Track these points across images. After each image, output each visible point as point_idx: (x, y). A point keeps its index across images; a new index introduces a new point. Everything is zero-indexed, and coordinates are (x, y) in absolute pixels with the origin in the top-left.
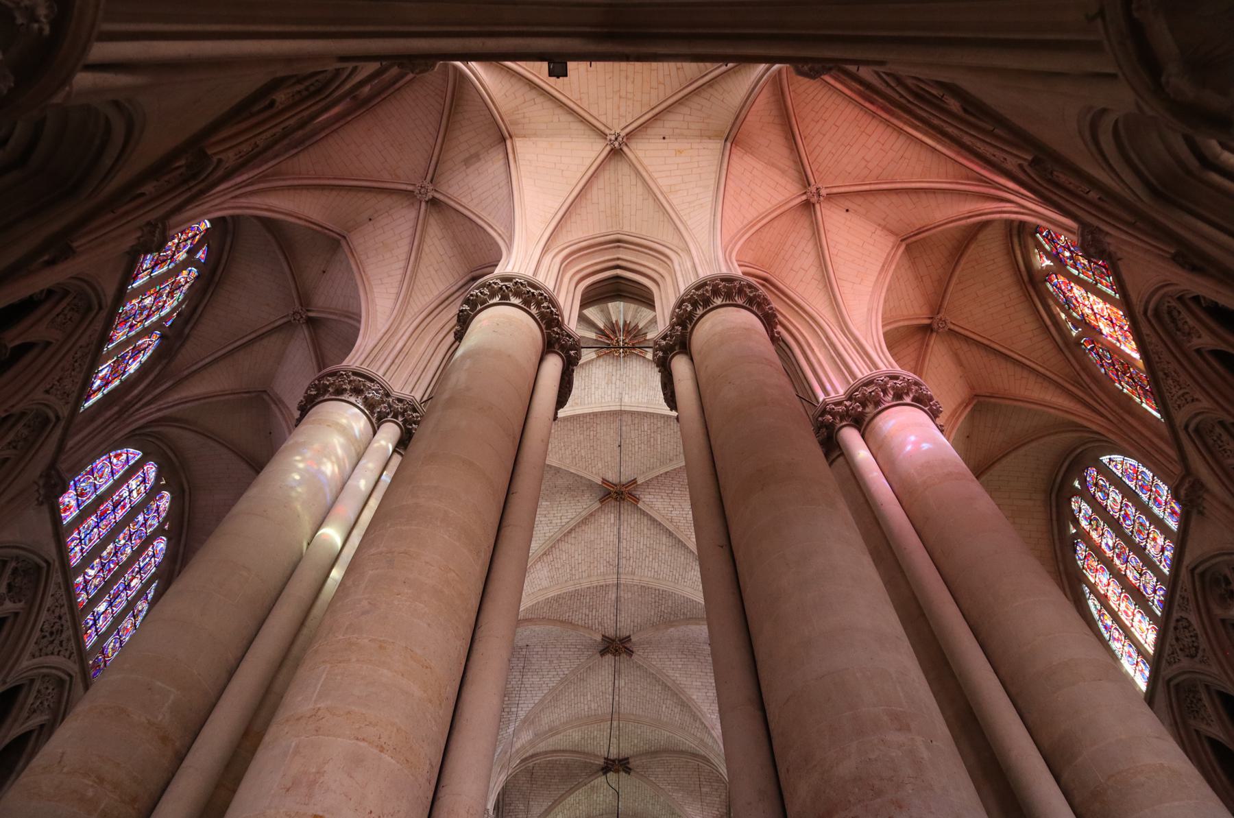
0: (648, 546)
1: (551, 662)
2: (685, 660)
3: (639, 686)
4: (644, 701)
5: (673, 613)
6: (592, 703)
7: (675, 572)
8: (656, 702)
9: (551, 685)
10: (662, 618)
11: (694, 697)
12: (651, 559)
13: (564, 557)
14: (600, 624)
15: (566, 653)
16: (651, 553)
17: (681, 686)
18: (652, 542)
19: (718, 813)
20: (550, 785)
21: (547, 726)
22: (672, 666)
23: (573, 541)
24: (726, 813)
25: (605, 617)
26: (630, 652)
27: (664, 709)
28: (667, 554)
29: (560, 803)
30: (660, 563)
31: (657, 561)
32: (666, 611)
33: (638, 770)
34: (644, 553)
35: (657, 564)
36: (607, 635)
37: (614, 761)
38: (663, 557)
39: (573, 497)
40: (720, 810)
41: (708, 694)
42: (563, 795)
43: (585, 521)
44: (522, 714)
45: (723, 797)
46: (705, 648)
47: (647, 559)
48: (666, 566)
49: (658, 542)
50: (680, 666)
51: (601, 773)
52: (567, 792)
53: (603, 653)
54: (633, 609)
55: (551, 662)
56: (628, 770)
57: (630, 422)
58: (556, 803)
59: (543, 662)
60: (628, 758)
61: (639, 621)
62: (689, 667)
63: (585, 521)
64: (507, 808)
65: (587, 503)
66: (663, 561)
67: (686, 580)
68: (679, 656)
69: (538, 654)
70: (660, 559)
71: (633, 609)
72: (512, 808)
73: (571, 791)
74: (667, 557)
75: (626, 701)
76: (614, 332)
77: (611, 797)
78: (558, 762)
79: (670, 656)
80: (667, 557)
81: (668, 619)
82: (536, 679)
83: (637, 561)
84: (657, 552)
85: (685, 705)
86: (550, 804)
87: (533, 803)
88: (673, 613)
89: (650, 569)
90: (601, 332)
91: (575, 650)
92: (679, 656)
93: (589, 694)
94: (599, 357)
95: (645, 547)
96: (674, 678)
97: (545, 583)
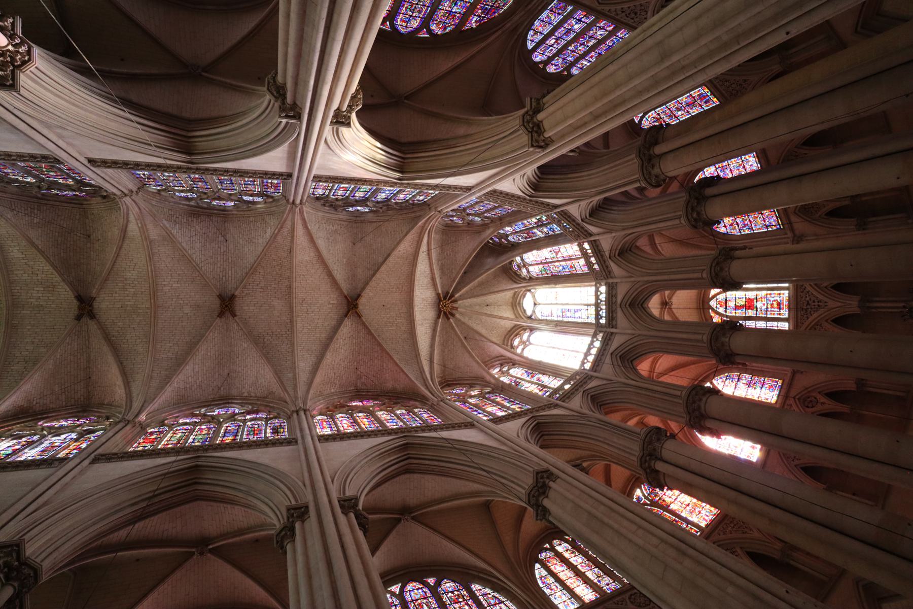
1: (211, 257)
6: (169, 288)
9: (194, 257)
11: (187, 367)
13: (313, 271)
14: (248, 294)
15: (218, 269)
17: (195, 356)
19: (34, 404)
20: (57, 248)
21: (157, 251)
22: (209, 348)
23: (322, 277)
24: (35, 412)
26: (221, 315)
29: (43, 256)
32: (265, 340)
33: (77, 327)
36: (237, 299)
37: (91, 306)
39: (349, 278)
40: (38, 405)
42: (50, 259)
43: (334, 282)
44: (174, 232)
45: (51, 406)
46: (226, 371)
50: (209, 354)
51: (77, 295)
52: (53, 263)
53: (220, 297)
54: (263, 317)
55: (211, 257)
56: (79, 318)
57: (401, 311)
58: (41, 252)
59: (211, 251)
60: (95, 318)
62: (209, 361)
63: (334, 282)
64: (36, 207)
65: (345, 286)
69: (218, 247)
71: (263, 317)
72: (36, 211)
73: (53, 265)
76: (451, 302)
77: (36, 303)
78: (82, 257)
79: (216, 346)
82: (198, 245)
85: (180, 362)
86: (40, 247)
87: (40, 231)
90: (452, 296)
91: (221, 276)
92: (217, 353)
93: (179, 285)
94: (438, 295)
96: (200, 350)
97: (299, 258)
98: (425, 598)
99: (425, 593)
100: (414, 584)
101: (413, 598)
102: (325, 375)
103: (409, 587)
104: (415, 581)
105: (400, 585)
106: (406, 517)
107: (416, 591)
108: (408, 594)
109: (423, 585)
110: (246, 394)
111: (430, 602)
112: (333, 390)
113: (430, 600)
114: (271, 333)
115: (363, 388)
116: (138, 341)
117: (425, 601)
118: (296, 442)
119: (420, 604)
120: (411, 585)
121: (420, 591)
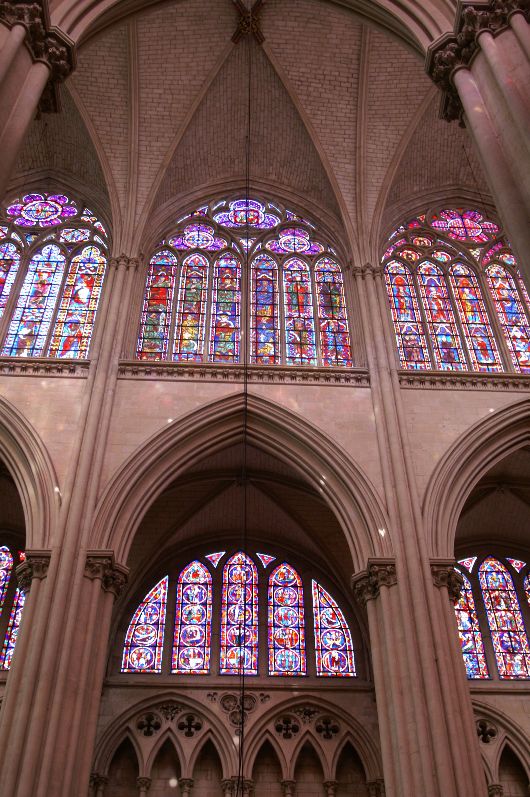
0: (405, 65)
2: (225, 110)
3: (181, 51)
4: (160, 61)
5: (311, 99)
7: (379, 103)
8: (163, 78)
10: (298, 83)
12: (389, 70)
16: (396, 69)
18: (409, 69)
22: (218, 95)
25: (295, 5)
27: (156, 91)
28: (397, 90)
30: (386, 82)
31: (388, 78)
32: (311, 89)
34: (396, 61)
35: (383, 78)
38: (393, 86)
41: (191, 148)
46: (242, 131)
47: (389, 65)
48: (383, 91)
49: (410, 77)
50: (218, 105)
61: (288, 51)
66: (388, 86)
67: (372, 120)
68: (229, 101)
70: (391, 82)
74: (393, 90)
75: (155, 34)
80: (393, 90)
81: (299, 92)
83: (387, 53)
84: (398, 77)
88: (311, 99)
89: (378, 70)
92: (229, 101)
95: (405, 60)
98: (504, 591)
99: (507, 582)
100: (494, 563)
101: (490, 585)
102: (407, 164)
103: (486, 566)
104: (497, 559)
105: (476, 558)
106: (503, 489)
107: (494, 574)
108: (484, 576)
109: (506, 568)
110: (273, 177)
111: (511, 599)
112: (415, 189)
113: (511, 596)
114: (322, 77)
115: (467, 182)
116: (111, 81)
117: (504, 595)
118: (368, 380)
119: (496, 598)
120: (490, 562)
121: (500, 576)
